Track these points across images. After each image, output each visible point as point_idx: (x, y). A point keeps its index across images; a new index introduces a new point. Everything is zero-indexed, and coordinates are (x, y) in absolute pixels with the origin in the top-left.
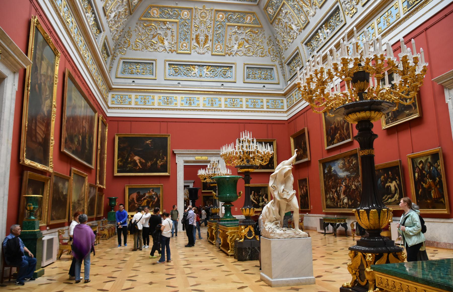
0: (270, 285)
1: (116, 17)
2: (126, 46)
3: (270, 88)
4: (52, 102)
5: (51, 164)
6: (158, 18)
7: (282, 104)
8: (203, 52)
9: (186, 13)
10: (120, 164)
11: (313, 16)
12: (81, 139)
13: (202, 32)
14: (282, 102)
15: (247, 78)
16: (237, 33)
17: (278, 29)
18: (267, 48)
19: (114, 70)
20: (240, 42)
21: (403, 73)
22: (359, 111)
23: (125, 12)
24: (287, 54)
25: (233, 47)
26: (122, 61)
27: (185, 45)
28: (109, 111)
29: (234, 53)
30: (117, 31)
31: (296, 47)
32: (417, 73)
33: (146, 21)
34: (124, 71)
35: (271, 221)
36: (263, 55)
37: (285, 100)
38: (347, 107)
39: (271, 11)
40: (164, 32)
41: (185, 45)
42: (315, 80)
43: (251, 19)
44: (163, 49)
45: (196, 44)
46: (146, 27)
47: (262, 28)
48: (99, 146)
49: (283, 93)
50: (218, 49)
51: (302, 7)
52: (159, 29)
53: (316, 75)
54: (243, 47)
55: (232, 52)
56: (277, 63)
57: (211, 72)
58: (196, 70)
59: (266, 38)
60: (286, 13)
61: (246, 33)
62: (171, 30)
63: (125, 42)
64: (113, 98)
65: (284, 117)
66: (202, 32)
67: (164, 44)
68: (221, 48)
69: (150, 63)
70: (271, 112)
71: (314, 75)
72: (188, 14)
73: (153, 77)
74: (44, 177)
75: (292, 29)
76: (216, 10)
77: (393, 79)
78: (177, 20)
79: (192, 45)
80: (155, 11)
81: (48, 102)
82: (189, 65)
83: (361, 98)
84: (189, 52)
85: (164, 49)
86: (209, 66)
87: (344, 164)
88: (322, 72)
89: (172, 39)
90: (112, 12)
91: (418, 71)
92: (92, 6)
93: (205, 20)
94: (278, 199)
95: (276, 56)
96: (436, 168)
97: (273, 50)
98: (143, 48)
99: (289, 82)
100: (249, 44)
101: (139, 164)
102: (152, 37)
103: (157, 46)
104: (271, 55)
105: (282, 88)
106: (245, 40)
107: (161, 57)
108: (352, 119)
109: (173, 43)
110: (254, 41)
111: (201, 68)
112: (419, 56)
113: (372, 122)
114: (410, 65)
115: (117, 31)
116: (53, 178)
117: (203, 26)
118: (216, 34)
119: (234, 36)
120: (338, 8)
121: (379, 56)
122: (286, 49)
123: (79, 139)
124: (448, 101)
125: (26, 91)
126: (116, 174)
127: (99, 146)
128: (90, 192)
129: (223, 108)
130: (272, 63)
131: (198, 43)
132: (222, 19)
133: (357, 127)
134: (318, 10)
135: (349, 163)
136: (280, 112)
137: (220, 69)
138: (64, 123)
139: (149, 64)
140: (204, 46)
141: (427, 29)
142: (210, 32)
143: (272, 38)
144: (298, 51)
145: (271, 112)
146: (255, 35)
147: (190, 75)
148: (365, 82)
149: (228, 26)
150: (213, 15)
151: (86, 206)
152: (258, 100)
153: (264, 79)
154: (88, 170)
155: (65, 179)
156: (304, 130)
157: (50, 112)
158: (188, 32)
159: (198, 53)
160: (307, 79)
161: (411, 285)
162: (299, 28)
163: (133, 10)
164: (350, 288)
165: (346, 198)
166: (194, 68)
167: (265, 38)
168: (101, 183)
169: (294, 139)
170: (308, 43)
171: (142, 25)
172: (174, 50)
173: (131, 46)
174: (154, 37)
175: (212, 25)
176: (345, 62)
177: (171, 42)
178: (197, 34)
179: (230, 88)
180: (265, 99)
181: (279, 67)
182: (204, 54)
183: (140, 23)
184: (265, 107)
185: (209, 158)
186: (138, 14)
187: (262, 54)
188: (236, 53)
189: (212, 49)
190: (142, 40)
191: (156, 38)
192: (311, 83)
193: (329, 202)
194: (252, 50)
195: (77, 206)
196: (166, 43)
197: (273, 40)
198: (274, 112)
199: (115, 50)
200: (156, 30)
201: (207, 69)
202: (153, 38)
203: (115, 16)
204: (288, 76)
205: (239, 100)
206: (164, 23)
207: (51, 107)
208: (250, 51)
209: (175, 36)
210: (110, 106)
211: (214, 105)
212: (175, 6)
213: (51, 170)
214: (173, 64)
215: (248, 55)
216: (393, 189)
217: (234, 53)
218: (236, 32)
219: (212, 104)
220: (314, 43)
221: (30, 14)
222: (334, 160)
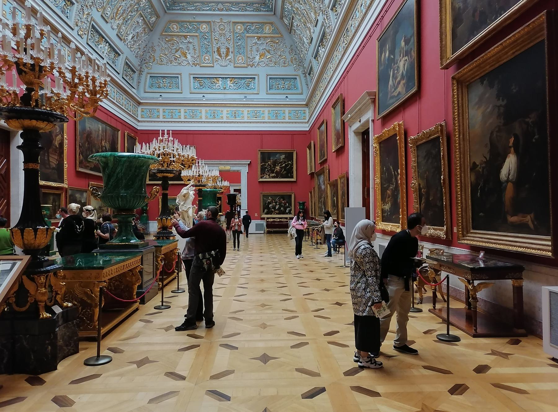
1: (136, 37)
3: (294, 99)
4: (63, 136)
5: (66, 182)
9: (204, 26)
26: (149, 76)
27: (207, 58)
28: (139, 124)
30: (139, 48)
34: (152, 86)
37: (307, 110)
41: (207, 58)
44: (187, 63)
45: (219, 58)
47: (282, 36)
56: (300, 72)
64: (143, 111)
65: (306, 127)
67: (187, 58)
69: (175, 77)
73: (180, 92)
79: (214, 58)
80: (175, 26)
81: (59, 137)
82: (213, 78)
84: (212, 65)
85: (187, 63)
89: (195, 52)
92: (103, 37)
97: (295, 59)
103: (181, 60)
107: (186, 71)
109: (195, 56)
115: (139, 48)
116: (70, 192)
131: (220, 55)
132: (240, 30)
137: (243, 81)
138: (78, 149)
139: (173, 79)
146: (275, 45)
147: (214, 87)
156: (311, 143)
157: (61, 144)
163: (152, 27)
166: (218, 81)
171: (164, 40)
173: (156, 61)
175: (232, 37)
177: (193, 55)
179: (252, 100)
180: (287, 110)
181: (302, 76)
182: (226, 66)
186: (159, 29)
188: (258, 65)
194: (274, 60)
196: (189, 56)
197: (294, 50)
206: (185, 37)
210: (140, 119)
212: (193, 20)
213: (66, 186)
214: (198, 78)
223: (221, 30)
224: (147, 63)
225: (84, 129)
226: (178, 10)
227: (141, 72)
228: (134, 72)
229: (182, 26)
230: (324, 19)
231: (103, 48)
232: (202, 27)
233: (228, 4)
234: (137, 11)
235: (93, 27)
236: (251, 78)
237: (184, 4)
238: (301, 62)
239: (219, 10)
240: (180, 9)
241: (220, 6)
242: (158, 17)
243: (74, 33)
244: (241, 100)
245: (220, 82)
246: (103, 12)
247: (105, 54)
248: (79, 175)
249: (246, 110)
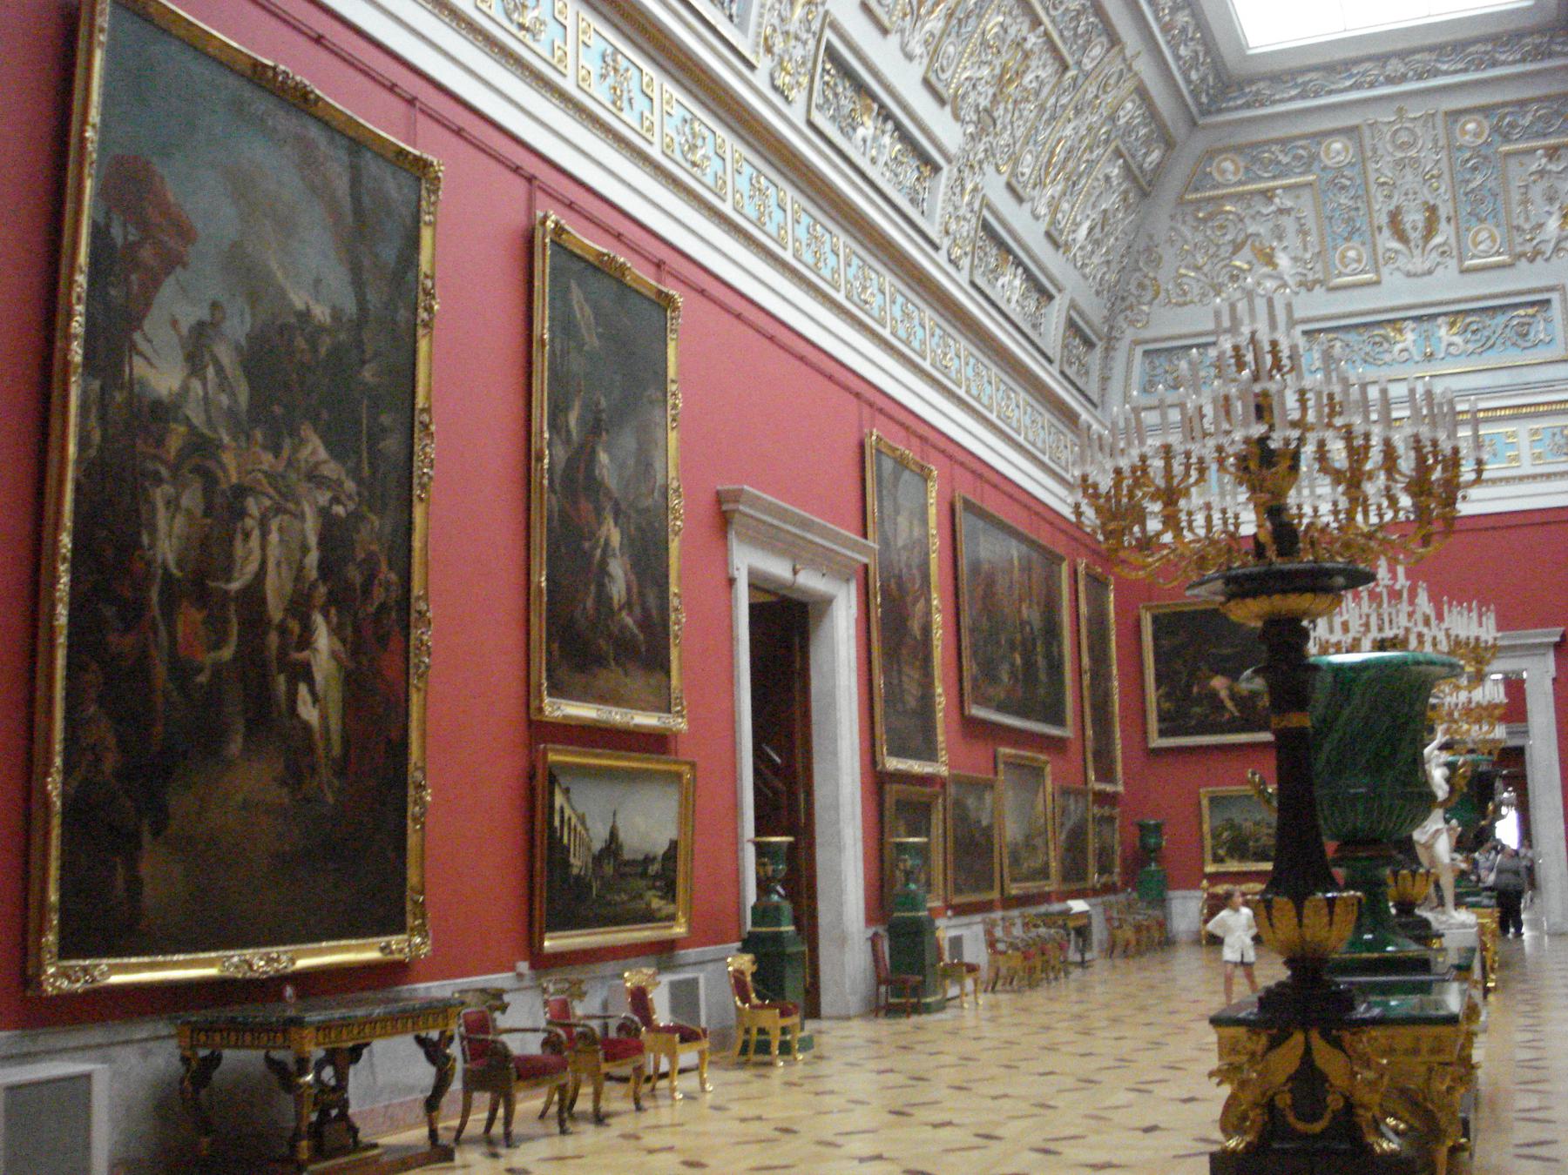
1: (1098, 229)
2: (1148, 298)
4: (928, 601)
5: (943, 756)
6: (1241, 183)
8: (1427, 266)
10: (1166, 705)
12: (1018, 661)
13: (1411, 197)
16: (1550, 172)
19: (1116, 386)
23: (1125, 200)
25: (1540, 226)
26: (1139, 351)
30: (1108, 262)
33: (1202, 203)
34: (1148, 387)
40: (1270, 224)
41: (1352, 254)
44: (1278, 283)
45: (1396, 245)
46: (1204, 220)
48: (1086, 660)
50: (1481, 247)
52: (1253, 217)
55: (1542, 247)
58: (1410, 337)
62: (1293, 214)
63: (1141, 286)
67: (1275, 266)
68: (1494, 241)
72: (1346, 149)
74: (927, 790)
76: (1447, 114)
78: (1311, 178)
79: (1380, 251)
80: (1228, 165)
81: (920, 605)
85: (1278, 283)
86: (1458, 313)
90: (1077, 225)
92: (1009, 251)
93: (1413, 153)
98: (1204, 295)
101: (1229, 704)
102: (1230, 249)
111: (1426, 326)
116: (952, 790)
117: (1409, 177)
118: (1466, 194)
119: (1543, 184)
123: (1013, 665)
125: (872, 606)
126: (1156, 742)
127: (1086, 660)
128: (1064, 810)
129: (1527, 468)
131: (1402, 237)
132: (1476, 135)
137: (1501, 319)
138: (965, 641)
142: (1442, 190)
147: (1387, 357)
149: (1508, 155)
150: (1441, 131)
151: (1052, 854)
154: (1055, 746)
155: (982, 786)
157: (927, 629)
158: (1357, 209)
159: (1409, 275)
166: (1400, 331)
168: (1106, 774)
171: (1189, 219)
172: (1316, 282)
173: (1162, 295)
174: (1237, 248)
175: (1444, 165)
177: (1300, 253)
178: (1392, 207)
182: (1430, 272)
183: (1184, 215)
190: (1198, 269)
191: (1246, 251)
195: (1024, 854)
196: (1283, 261)
199: (1106, 319)
200: (1240, 226)
202: (1234, 253)
203: (1091, 230)
207: (928, 613)
209: (1314, 231)
213: (943, 771)
218: (1542, 173)
221: (861, 427)
223: (1402, 146)
224: (1131, 307)
225: (975, 568)
226: (1237, 108)
227: (1110, 341)
228: (1089, 344)
229: (1254, 160)
231: (1010, 286)
232: (1328, 148)
233: (1426, 56)
234: (1107, 141)
235: (986, 226)
236: (1532, 304)
237: (1262, 85)
239: (1390, 80)
240: (1248, 106)
241: (1395, 67)
242: (1169, 144)
243: (941, 257)
245: (1410, 336)
246: (1013, 174)
247: (1013, 304)
248: (974, 729)
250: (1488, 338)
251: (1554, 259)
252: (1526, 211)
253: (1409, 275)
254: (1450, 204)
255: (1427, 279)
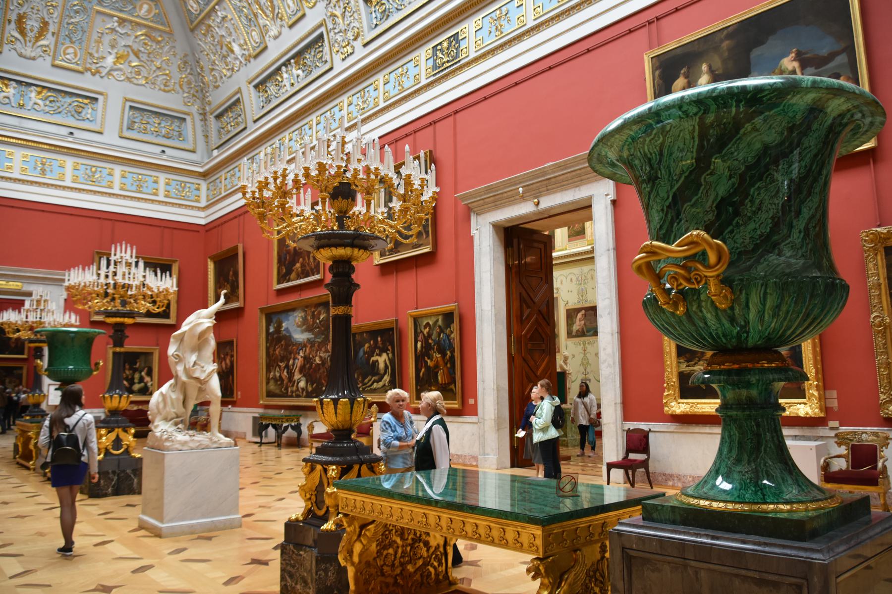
0: (159, 536)
3: (174, 158)
7: (196, 193)
8: (33, 54)
11: (276, 38)
13: (35, 11)
14: (198, 189)
15: (129, 128)
16: (117, 31)
17: (204, 44)
18: (177, 76)
20: (120, 52)
21: (404, 198)
22: (336, 246)
24: (219, 97)
25: (103, 58)
29: (104, 72)
31: (235, 88)
32: (423, 198)
35: (166, 419)
36: (166, 89)
37: (204, 186)
38: (319, 237)
39: (195, 6)
42: (272, 186)
43: (149, 11)
45: (19, 37)
47: (170, 33)
49: (201, 170)
50: (68, 56)
51: (256, 15)
53: (275, 179)
54: (127, 64)
55: (101, 70)
56: (195, 109)
57: (48, 103)
59: (178, 57)
60: (223, 18)
61: (136, 37)
65: (200, 218)
66: (35, 11)
68: (76, 56)
70: (173, 204)
71: (271, 180)
75: (232, 51)
77: (391, 201)
83: (341, 226)
87: (305, 319)
88: (284, 176)
91: (426, 197)
94: (184, 378)
95: (194, 96)
96: (448, 336)
97: (189, 83)
99: (215, 153)
100: (141, 61)
104: (184, 92)
105: (200, 161)
106: (133, 50)
108: (325, 256)
110: (151, 56)
111: (23, 88)
112: (427, 177)
113: (354, 263)
114: (415, 187)
118: (68, 24)
120: (321, 36)
121: (372, 168)
122: (217, 87)
124: (473, 232)
129: (68, 183)
130: (185, 109)
131: (22, 32)
133: (331, 268)
134: (285, 30)
135: (313, 316)
136: (192, 207)
137: (69, 100)
140: (37, 41)
141: (456, 112)
142: (55, 16)
143: (190, 59)
144: (239, 95)
145: (173, 204)
148: (350, 200)
149: (98, 12)
152: (148, 178)
153: (164, 136)
156: (236, 248)
159: (21, 55)
160: (260, 182)
161: (385, 504)
162: (246, 53)
164: (301, 521)
165: (304, 379)
166: (7, 86)
167: (175, 55)
169: (215, 263)
170: (261, 86)
176: (321, 167)
179: (89, 142)
180: (162, 177)
181: (198, 118)
182: (34, 59)
184: (162, 192)
185: (25, 285)
187: (165, 86)
189: (55, 52)
192: (265, 190)
193: (272, 386)
194: (144, 72)
198: (180, 205)
201: (39, 93)
204: (215, 141)
205: (106, 172)
208: (139, 75)
211: (48, 173)
215: (135, 81)
216: (382, 366)
217: (104, 72)
218: (113, 30)
219: (43, 172)
220: (272, 89)
222: (289, 310)
230: (334, 16)
238: (200, 92)
244: (61, 137)
249: (69, 162)
250: (59, 107)
251: (106, 78)
252: (98, 47)
253: (21, 55)
254: (56, 25)
255: (31, 61)
